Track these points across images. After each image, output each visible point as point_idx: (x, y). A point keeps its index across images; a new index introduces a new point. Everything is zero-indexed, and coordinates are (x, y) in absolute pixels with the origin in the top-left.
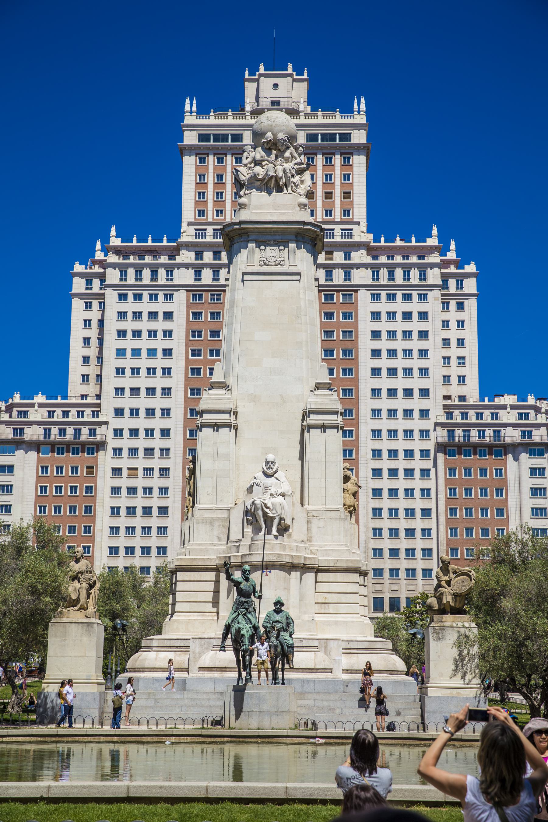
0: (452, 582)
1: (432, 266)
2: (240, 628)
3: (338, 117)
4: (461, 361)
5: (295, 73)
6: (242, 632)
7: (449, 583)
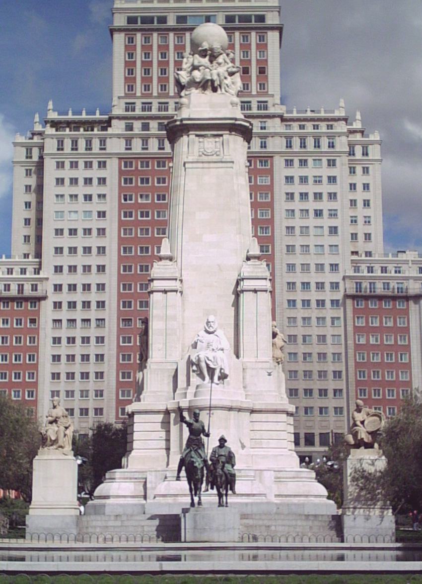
0: (366, 423)
2: (193, 461)
6: (195, 465)
7: (362, 422)
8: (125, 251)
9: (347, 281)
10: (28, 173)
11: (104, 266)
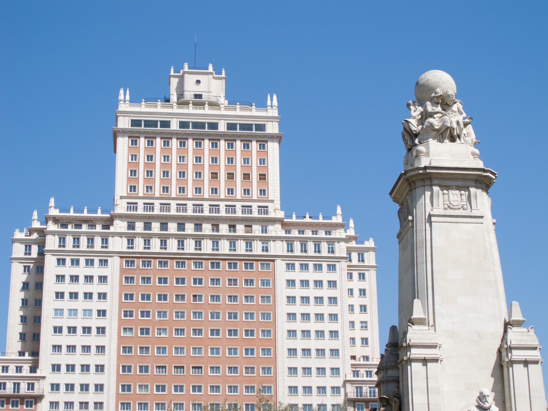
1: (339, 240)
3: (254, 110)
4: (364, 325)
5: (214, 72)
8: (125, 351)
9: (348, 386)
10: (26, 269)
11: (103, 366)
